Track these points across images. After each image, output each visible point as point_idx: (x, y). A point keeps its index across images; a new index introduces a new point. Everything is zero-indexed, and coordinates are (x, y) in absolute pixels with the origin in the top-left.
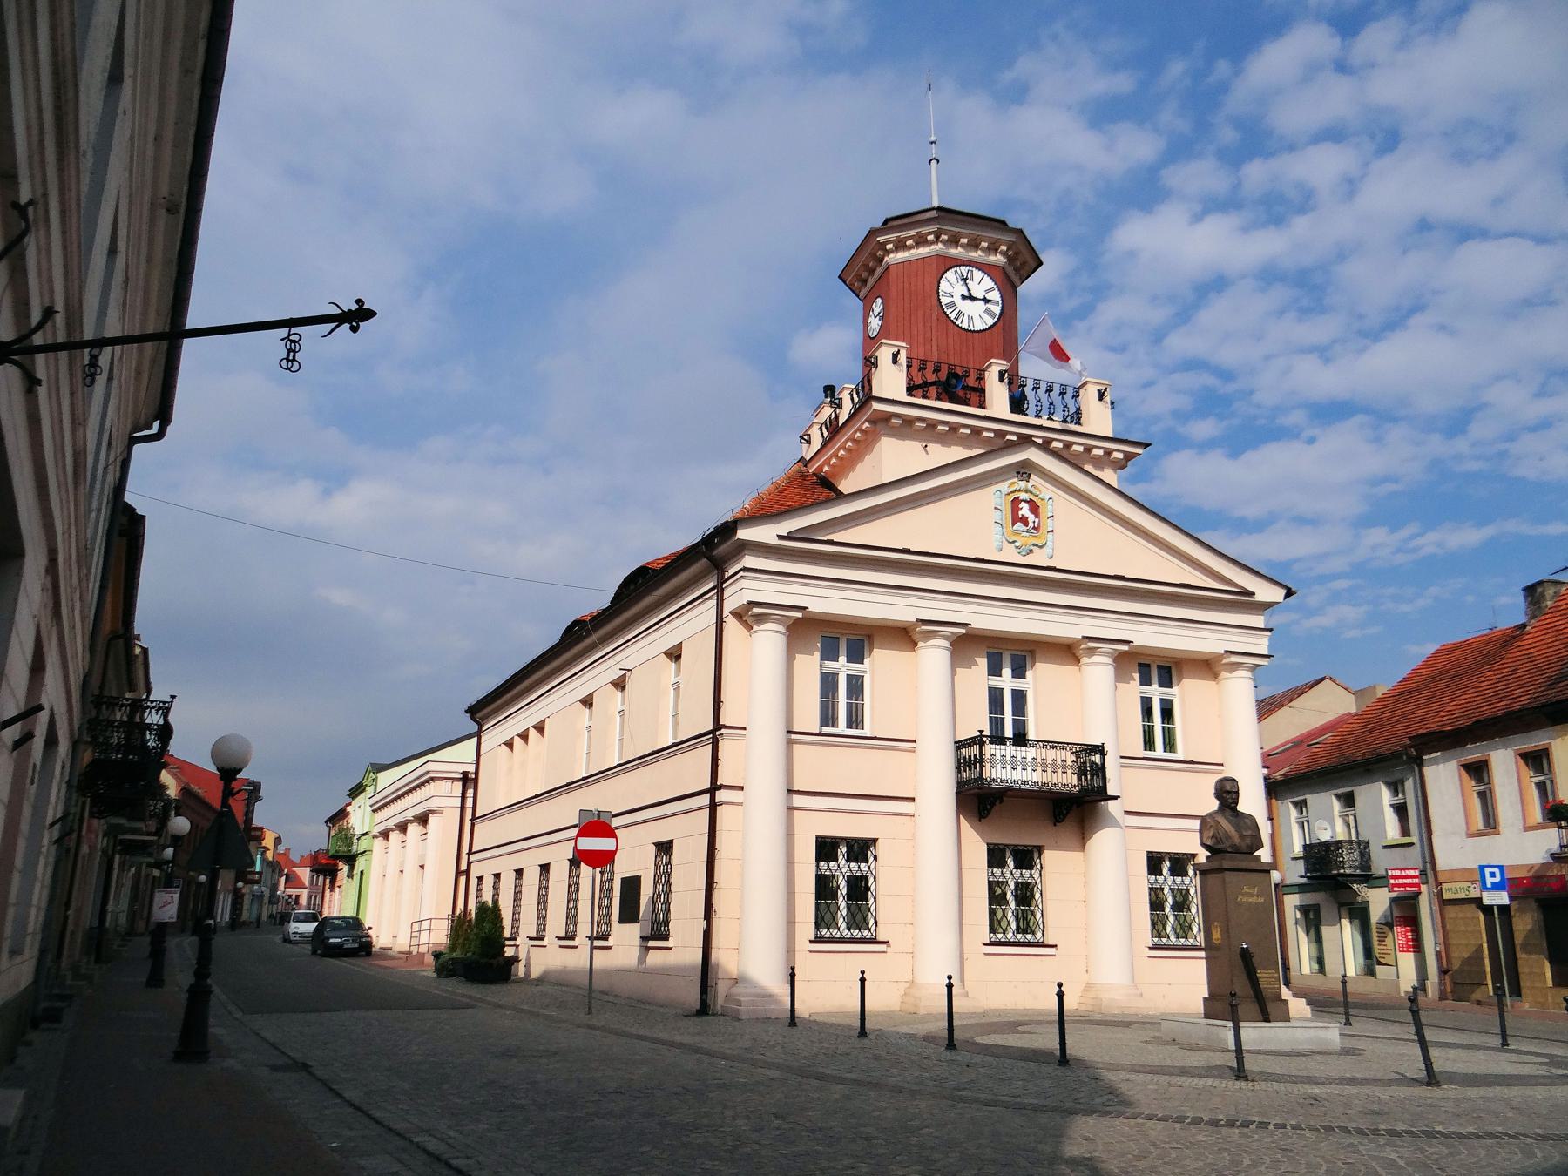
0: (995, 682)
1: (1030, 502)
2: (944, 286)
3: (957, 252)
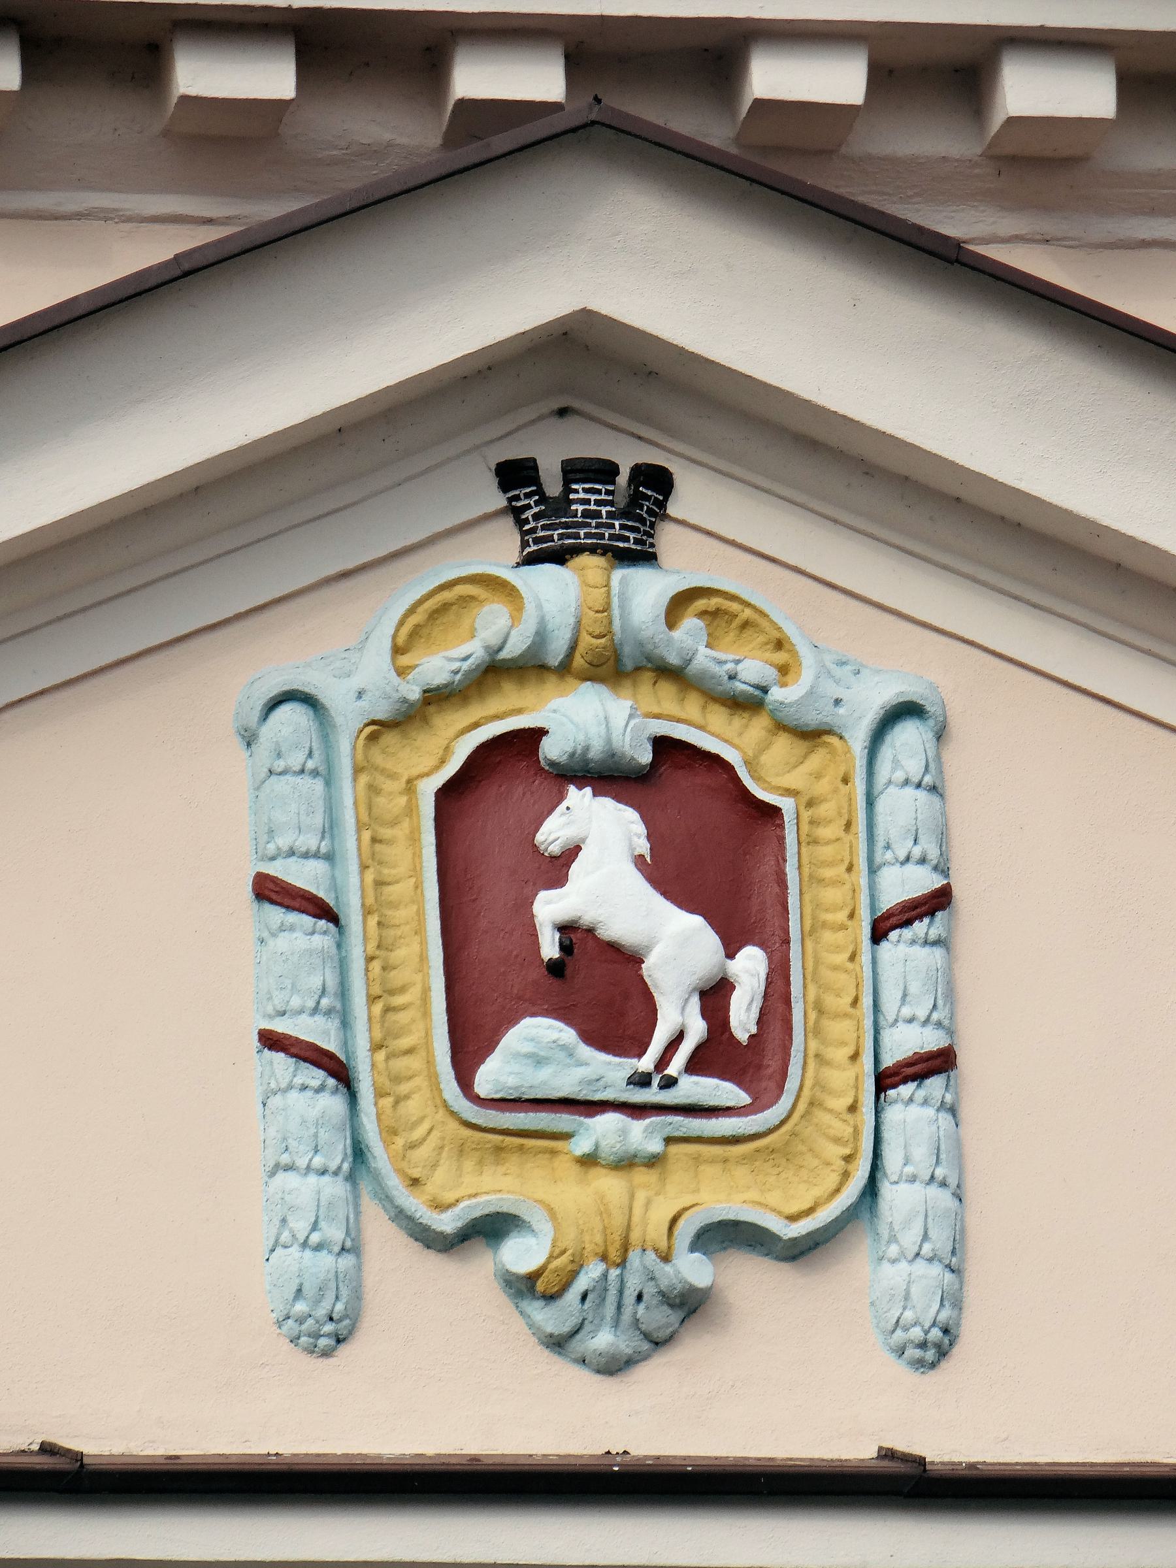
1: (661, 777)
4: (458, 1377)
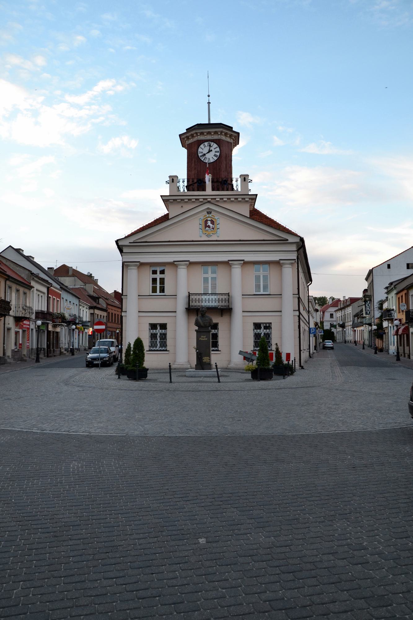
0: (206, 276)
2: (200, 150)
3: (202, 138)
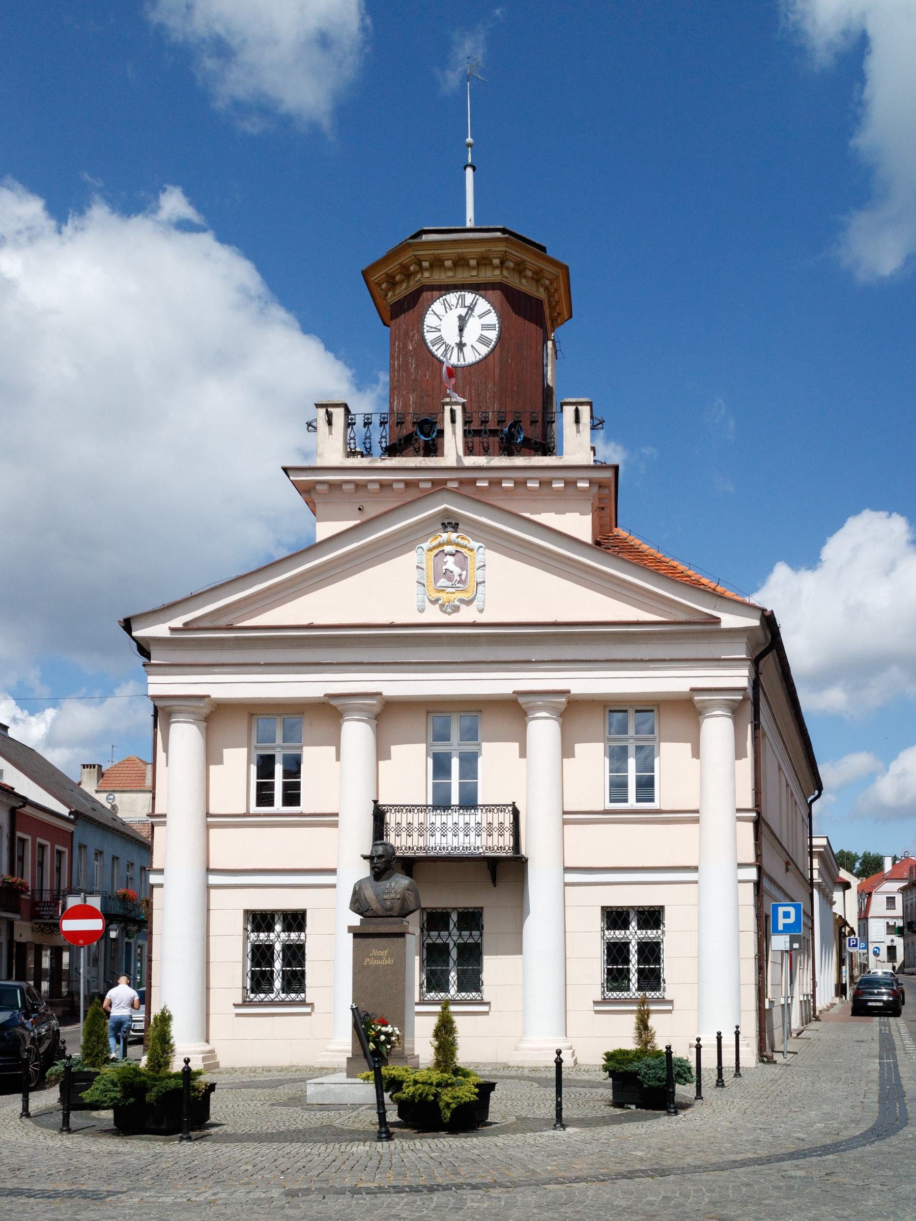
2: (430, 320)
3: (440, 277)
4: (434, 615)
